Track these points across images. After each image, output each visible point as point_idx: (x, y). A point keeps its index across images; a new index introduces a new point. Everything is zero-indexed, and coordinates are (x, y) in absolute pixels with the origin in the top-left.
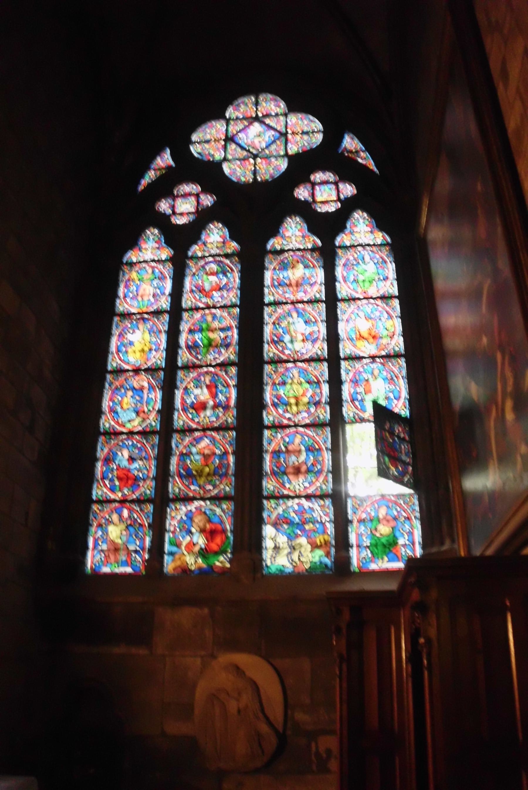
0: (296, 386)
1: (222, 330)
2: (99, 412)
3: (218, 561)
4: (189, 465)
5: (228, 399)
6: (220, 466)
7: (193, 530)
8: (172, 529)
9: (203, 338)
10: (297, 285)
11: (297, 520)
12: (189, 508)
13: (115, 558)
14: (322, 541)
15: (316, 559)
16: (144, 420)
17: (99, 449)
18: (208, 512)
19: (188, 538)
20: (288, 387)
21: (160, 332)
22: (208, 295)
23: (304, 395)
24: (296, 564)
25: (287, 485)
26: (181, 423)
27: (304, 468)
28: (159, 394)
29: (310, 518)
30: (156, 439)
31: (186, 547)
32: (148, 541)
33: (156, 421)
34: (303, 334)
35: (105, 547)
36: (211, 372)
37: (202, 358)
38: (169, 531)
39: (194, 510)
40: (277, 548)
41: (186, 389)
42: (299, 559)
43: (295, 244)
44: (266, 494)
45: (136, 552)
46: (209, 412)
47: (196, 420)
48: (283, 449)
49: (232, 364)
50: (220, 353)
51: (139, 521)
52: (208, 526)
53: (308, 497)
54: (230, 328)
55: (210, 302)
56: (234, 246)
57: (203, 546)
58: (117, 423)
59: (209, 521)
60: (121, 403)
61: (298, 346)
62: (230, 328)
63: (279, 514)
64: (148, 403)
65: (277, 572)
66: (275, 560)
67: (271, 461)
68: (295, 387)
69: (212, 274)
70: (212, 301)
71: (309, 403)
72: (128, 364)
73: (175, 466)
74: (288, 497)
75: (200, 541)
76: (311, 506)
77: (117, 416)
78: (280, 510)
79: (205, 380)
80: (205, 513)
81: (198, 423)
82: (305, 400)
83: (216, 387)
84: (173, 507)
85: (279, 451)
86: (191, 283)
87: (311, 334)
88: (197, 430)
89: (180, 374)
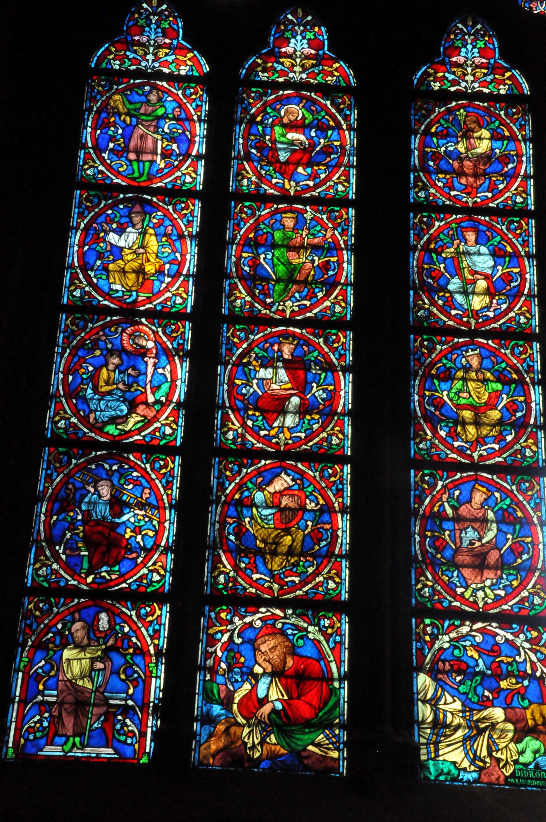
0: (474, 385)
1: (315, 248)
2: (45, 397)
3: (313, 744)
4: (248, 526)
5: (333, 396)
6: (315, 536)
7: (258, 670)
8: (210, 662)
9: (276, 261)
10: (476, 176)
11: (481, 666)
12: (248, 620)
13: (75, 724)
14: (537, 716)
15: (527, 757)
16: (147, 422)
17: (42, 475)
18: (289, 632)
19: (247, 687)
20: (458, 385)
21: (181, 237)
22: (286, 170)
23: (491, 405)
24: (485, 763)
25: (459, 591)
26: (230, 435)
27: (493, 557)
28: (183, 370)
29: (510, 664)
30: (176, 465)
31: (239, 704)
32: (156, 685)
33: (174, 426)
34: (487, 277)
35: (51, 696)
36: (294, 335)
37: (273, 303)
38: (204, 668)
39: (259, 624)
40: (439, 725)
41: (238, 364)
42: (490, 754)
43: (470, 83)
44: (413, 601)
45: (126, 710)
46: (290, 420)
47: (262, 433)
48: (449, 511)
49: (341, 325)
50: (311, 295)
51: (134, 640)
52: (290, 663)
53: (505, 620)
54: (335, 248)
55: (291, 187)
56: (339, 72)
57: (279, 706)
58: (85, 420)
59: (293, 651)
60: (94, 378)
61: (477, 303)
62: (335, 248)
63: (441, 649)
64: (155, 389)
65: (442, 778)
66: (437, 750)
67: (423, 537)
68: (471, 385)
69: (292, 126)
70: (293, 184)
71: (500, 422)
72: (107, 295)
73: (217, 526)
74: (463, 616)
75: (273, 693)
76: (510, 637)
77: (85, 407)
78: (444, 642)
79: (280, 350)
80: (282, 632)
81: (266, 440)
82: (495, 415)
83: (308, 369)
84: (213, 615)
85: (442, 516)
86: (246, 139)
87: (507, 278)
88: (265, 455)
89: (226, 332)
